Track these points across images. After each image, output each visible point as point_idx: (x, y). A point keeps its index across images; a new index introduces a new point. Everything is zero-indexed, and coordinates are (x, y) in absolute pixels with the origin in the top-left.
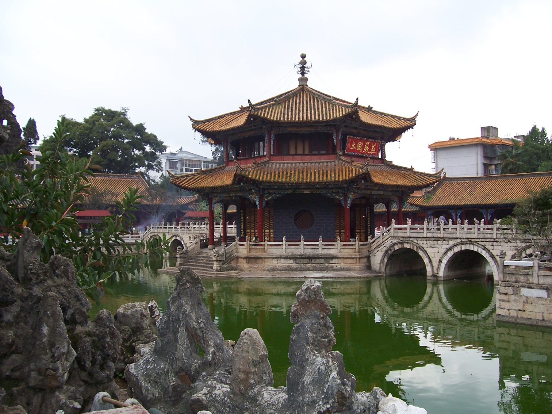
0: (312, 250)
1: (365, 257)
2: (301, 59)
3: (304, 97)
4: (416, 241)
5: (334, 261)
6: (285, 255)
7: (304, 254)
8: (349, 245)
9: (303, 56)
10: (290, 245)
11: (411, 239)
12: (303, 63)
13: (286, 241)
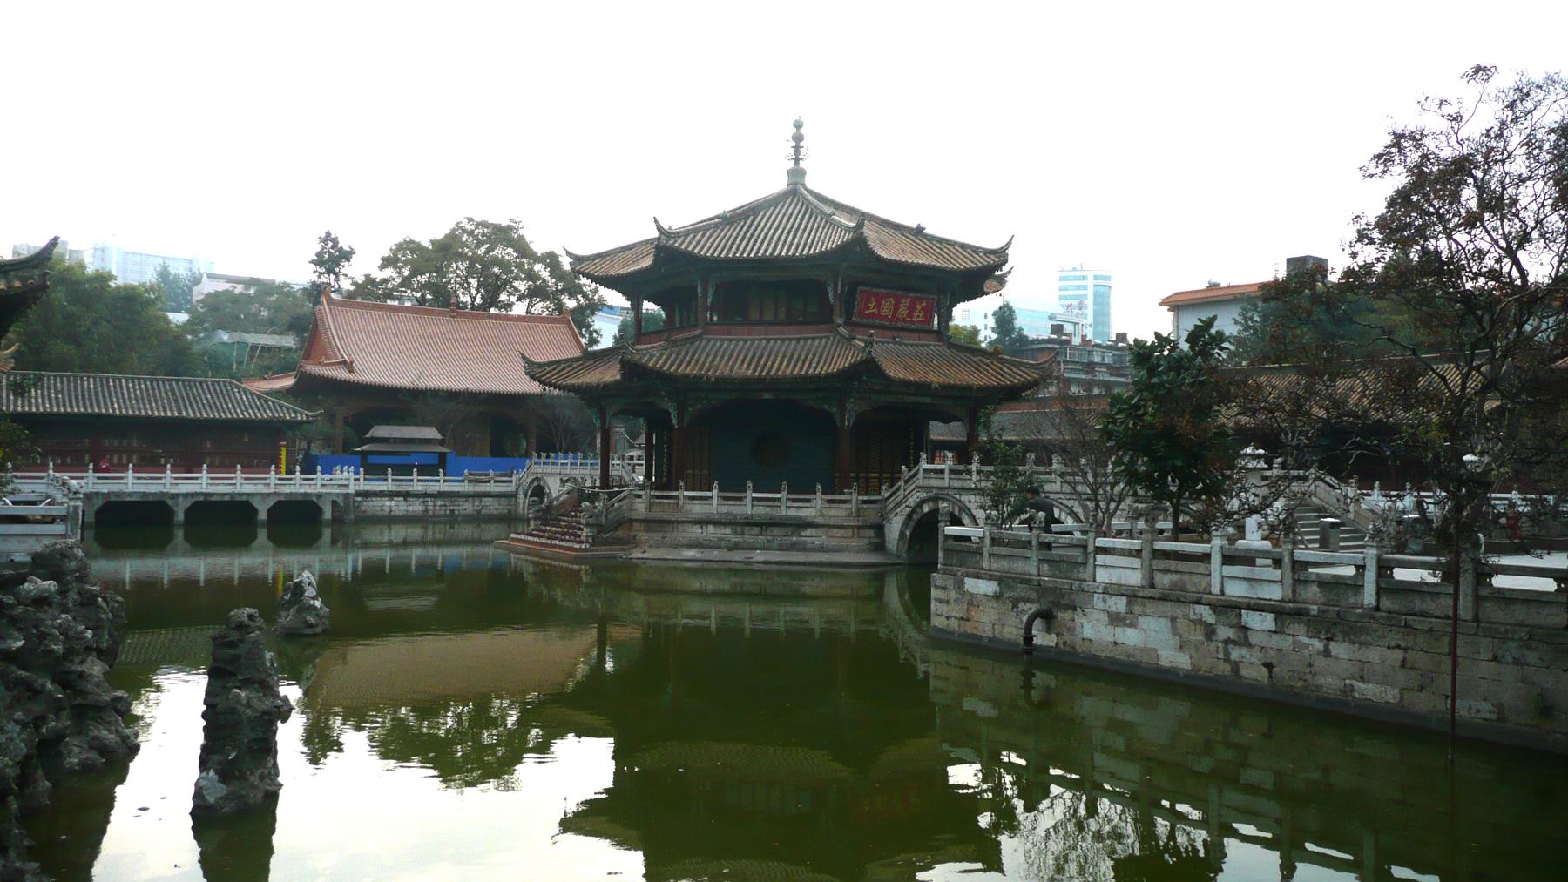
1: (871, 527)
2: (794, 130)
3: (792, 207)
5: (809, 532)
8: (841, 502)
9: (798, 125)
12: (798, 138)
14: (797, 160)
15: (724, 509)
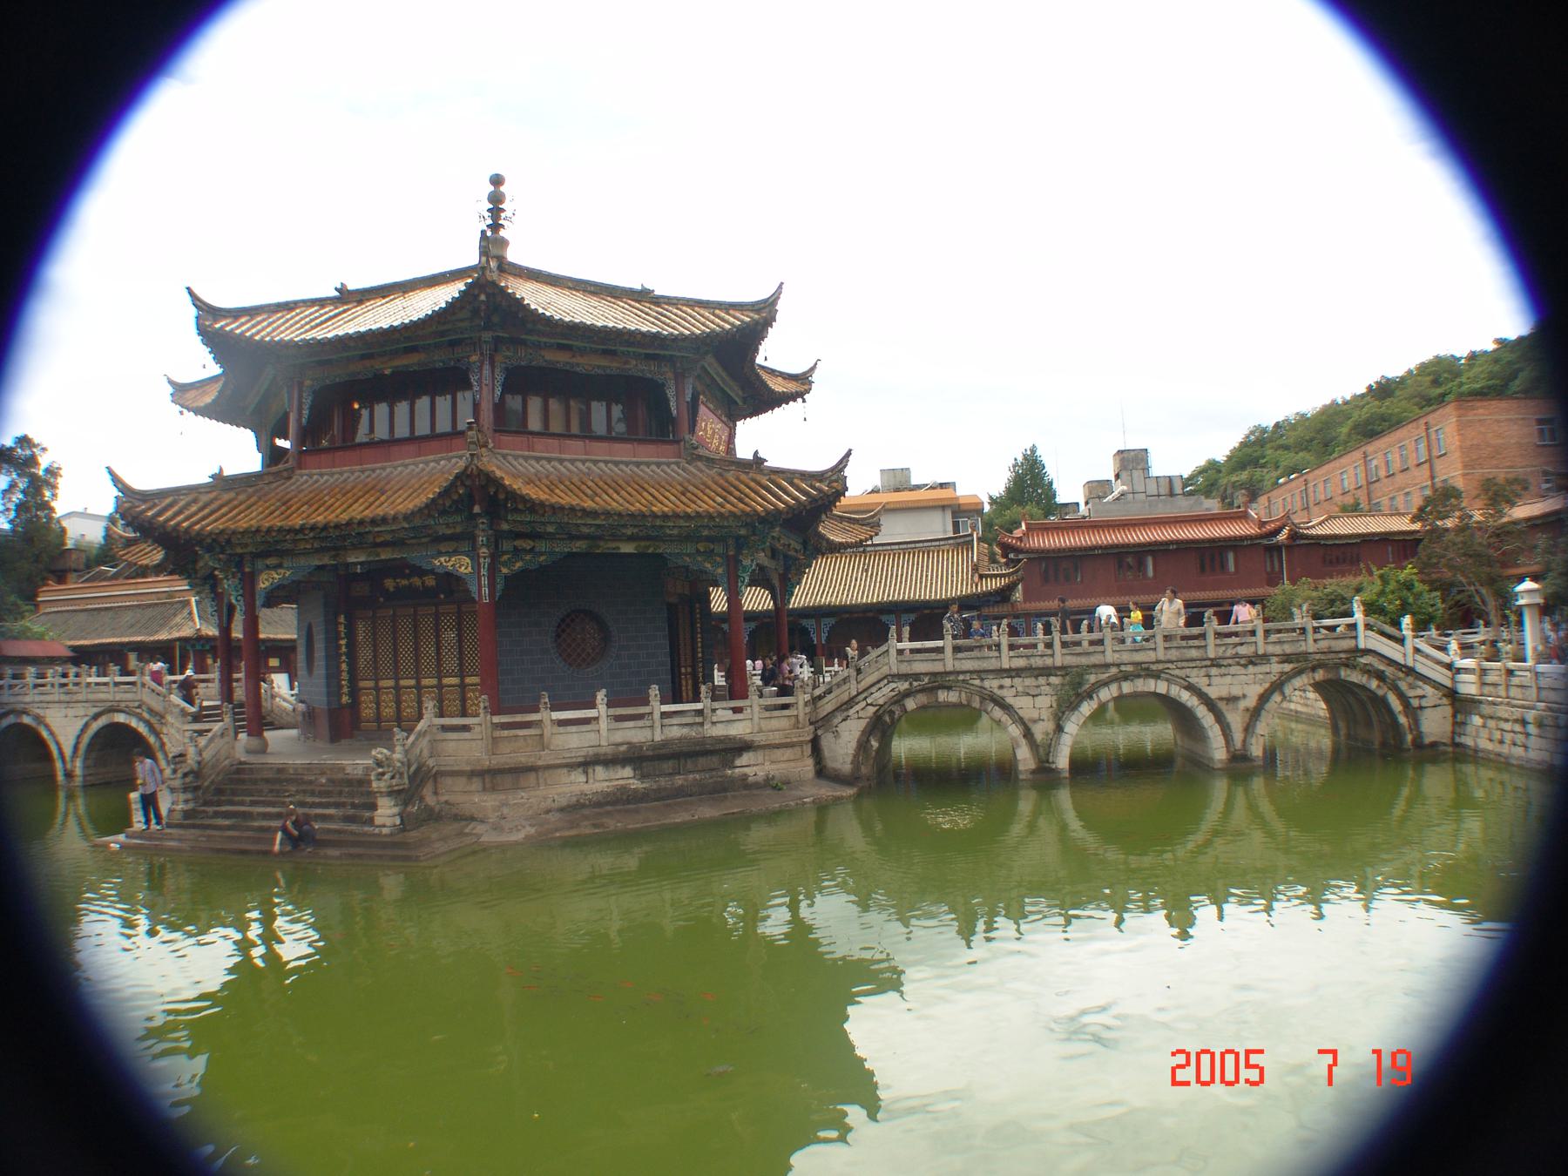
0: (685, 731)
2: (492, 188)
4: (977, 682)
5: (746, 758)
6: (607, 750)
7: (665, 743)
9: (497, 181)
10: (619, 719)
11: (961, 677)
12: (496, 200)
13: (609, 705)
14: (496, 227)
15: (619, 737)
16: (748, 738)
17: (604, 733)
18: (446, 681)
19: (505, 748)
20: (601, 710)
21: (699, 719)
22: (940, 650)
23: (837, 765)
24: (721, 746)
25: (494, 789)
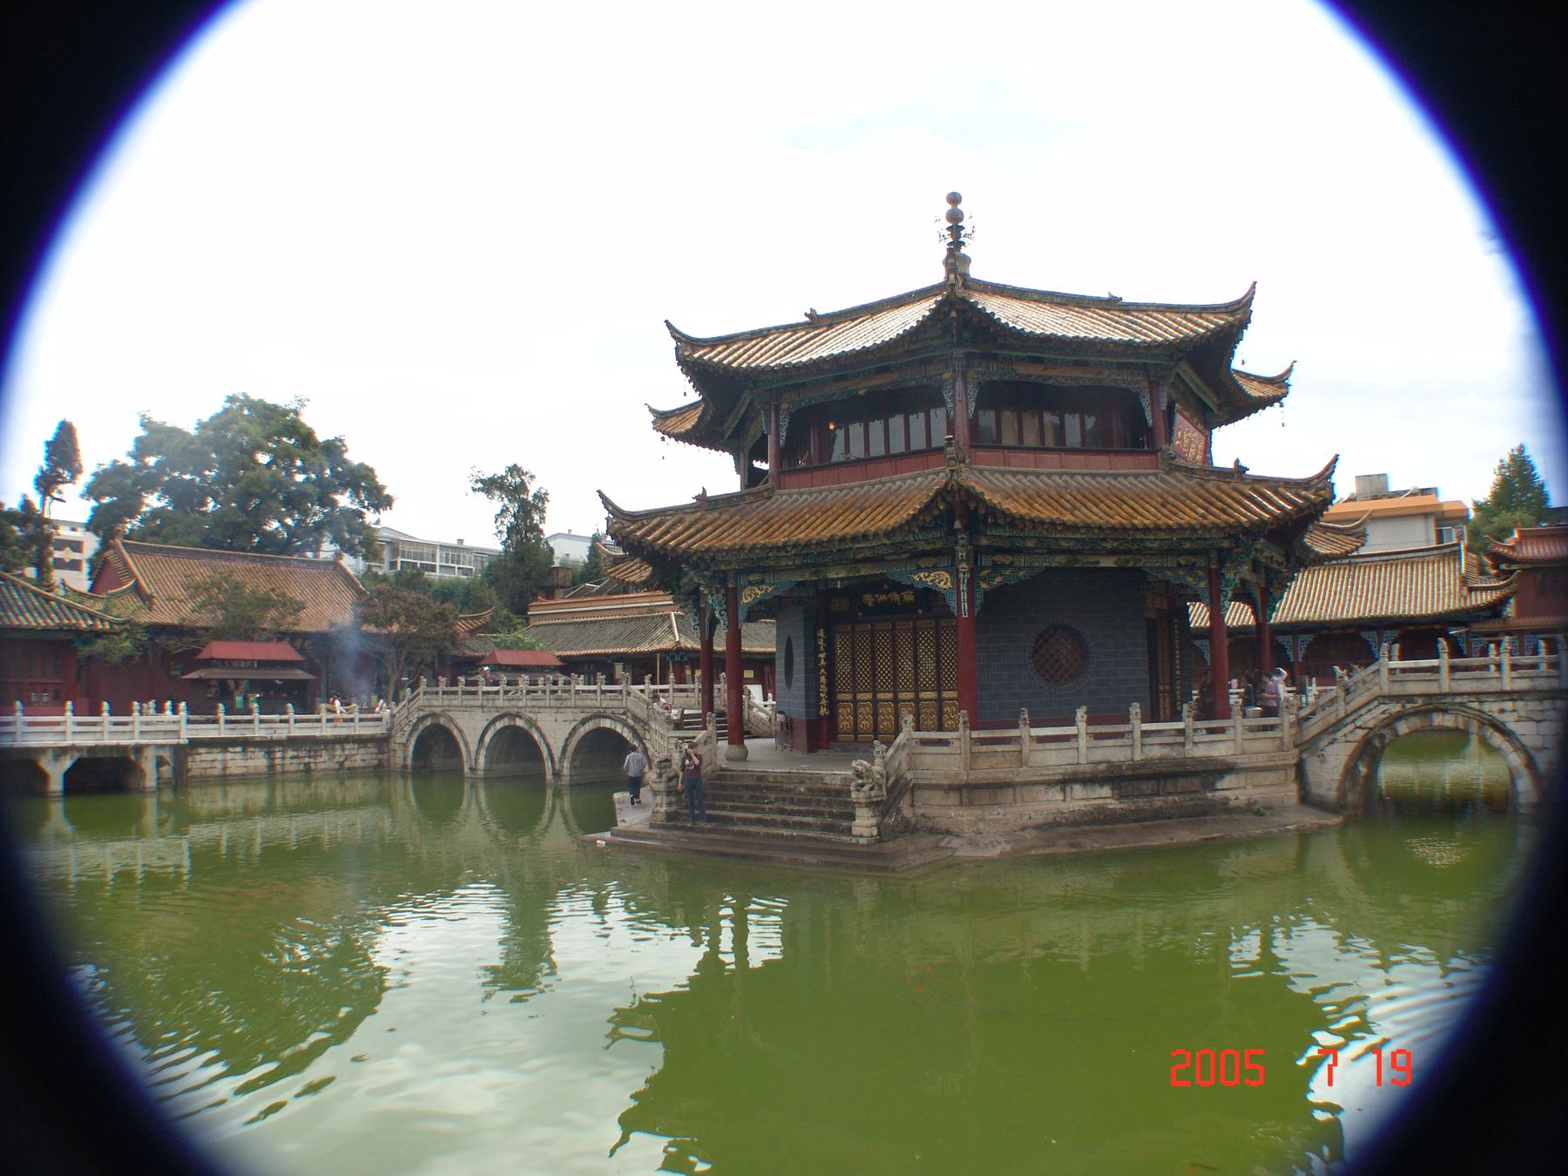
0: (1166, 751)
2: (949, 207)
4: (1475, 705)
5: (1227, 781)
7: (1146, 763)
9: (954, 199)
10: (1099, 736)
11: (1458, 700)
12: (955, 218)
13: (1089, 722)
14: (956, 245)
15: (1098, 755)
16: (1231, 759)
17: (1083, 750)
18: (923, 695)
19: (983, 763)
20: (1081, 727)
21: (1180, 739)
22: (1435, 670)
23: (1322, 792)
24: (1200, 768)
25: (971, 804)
